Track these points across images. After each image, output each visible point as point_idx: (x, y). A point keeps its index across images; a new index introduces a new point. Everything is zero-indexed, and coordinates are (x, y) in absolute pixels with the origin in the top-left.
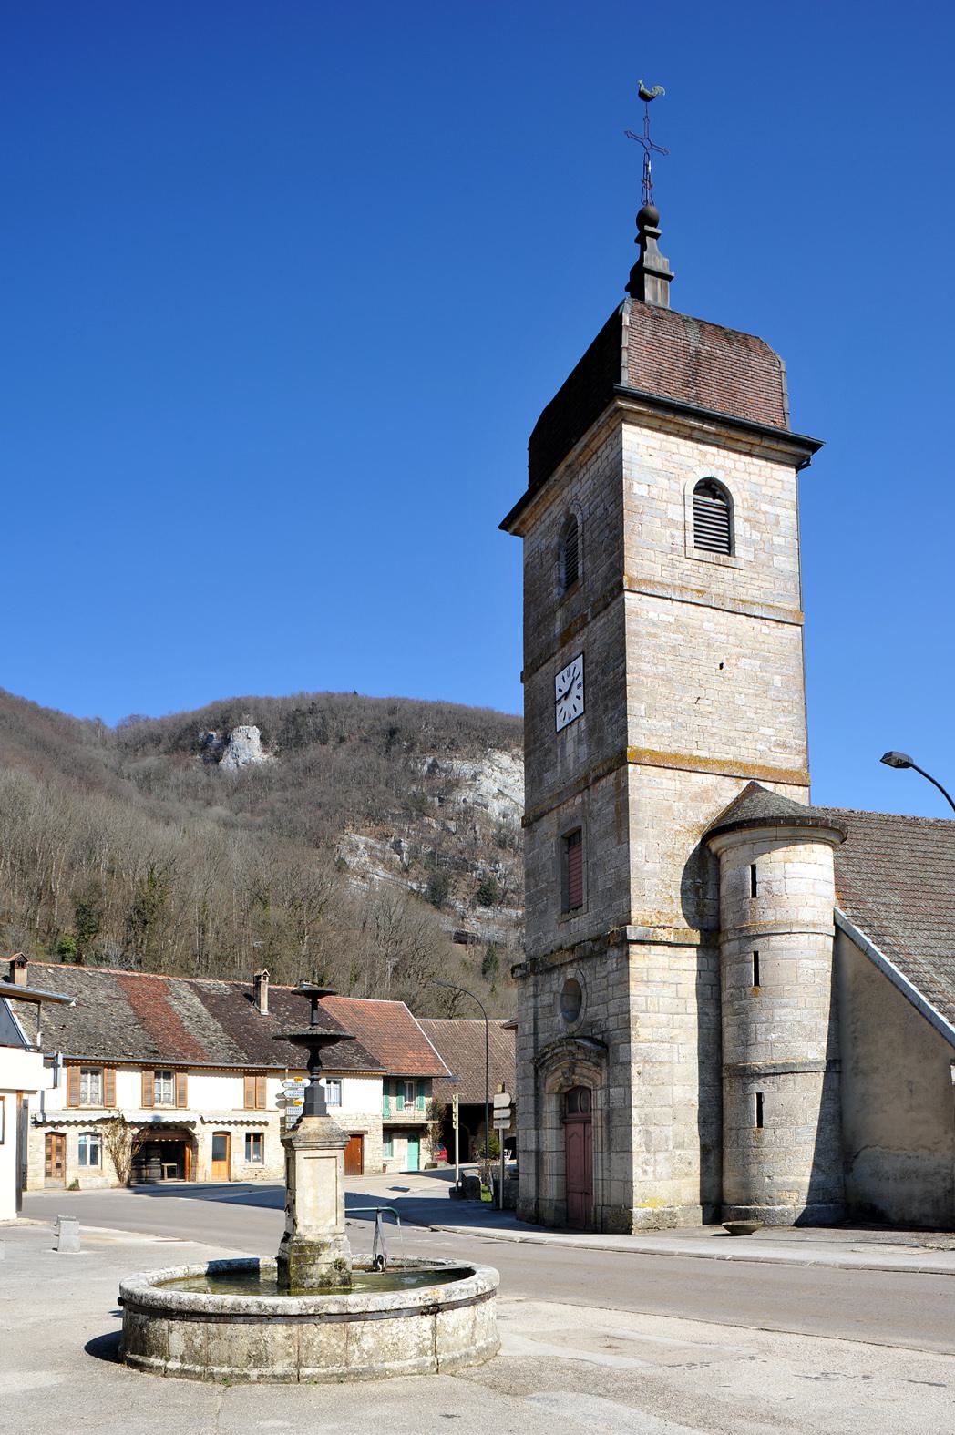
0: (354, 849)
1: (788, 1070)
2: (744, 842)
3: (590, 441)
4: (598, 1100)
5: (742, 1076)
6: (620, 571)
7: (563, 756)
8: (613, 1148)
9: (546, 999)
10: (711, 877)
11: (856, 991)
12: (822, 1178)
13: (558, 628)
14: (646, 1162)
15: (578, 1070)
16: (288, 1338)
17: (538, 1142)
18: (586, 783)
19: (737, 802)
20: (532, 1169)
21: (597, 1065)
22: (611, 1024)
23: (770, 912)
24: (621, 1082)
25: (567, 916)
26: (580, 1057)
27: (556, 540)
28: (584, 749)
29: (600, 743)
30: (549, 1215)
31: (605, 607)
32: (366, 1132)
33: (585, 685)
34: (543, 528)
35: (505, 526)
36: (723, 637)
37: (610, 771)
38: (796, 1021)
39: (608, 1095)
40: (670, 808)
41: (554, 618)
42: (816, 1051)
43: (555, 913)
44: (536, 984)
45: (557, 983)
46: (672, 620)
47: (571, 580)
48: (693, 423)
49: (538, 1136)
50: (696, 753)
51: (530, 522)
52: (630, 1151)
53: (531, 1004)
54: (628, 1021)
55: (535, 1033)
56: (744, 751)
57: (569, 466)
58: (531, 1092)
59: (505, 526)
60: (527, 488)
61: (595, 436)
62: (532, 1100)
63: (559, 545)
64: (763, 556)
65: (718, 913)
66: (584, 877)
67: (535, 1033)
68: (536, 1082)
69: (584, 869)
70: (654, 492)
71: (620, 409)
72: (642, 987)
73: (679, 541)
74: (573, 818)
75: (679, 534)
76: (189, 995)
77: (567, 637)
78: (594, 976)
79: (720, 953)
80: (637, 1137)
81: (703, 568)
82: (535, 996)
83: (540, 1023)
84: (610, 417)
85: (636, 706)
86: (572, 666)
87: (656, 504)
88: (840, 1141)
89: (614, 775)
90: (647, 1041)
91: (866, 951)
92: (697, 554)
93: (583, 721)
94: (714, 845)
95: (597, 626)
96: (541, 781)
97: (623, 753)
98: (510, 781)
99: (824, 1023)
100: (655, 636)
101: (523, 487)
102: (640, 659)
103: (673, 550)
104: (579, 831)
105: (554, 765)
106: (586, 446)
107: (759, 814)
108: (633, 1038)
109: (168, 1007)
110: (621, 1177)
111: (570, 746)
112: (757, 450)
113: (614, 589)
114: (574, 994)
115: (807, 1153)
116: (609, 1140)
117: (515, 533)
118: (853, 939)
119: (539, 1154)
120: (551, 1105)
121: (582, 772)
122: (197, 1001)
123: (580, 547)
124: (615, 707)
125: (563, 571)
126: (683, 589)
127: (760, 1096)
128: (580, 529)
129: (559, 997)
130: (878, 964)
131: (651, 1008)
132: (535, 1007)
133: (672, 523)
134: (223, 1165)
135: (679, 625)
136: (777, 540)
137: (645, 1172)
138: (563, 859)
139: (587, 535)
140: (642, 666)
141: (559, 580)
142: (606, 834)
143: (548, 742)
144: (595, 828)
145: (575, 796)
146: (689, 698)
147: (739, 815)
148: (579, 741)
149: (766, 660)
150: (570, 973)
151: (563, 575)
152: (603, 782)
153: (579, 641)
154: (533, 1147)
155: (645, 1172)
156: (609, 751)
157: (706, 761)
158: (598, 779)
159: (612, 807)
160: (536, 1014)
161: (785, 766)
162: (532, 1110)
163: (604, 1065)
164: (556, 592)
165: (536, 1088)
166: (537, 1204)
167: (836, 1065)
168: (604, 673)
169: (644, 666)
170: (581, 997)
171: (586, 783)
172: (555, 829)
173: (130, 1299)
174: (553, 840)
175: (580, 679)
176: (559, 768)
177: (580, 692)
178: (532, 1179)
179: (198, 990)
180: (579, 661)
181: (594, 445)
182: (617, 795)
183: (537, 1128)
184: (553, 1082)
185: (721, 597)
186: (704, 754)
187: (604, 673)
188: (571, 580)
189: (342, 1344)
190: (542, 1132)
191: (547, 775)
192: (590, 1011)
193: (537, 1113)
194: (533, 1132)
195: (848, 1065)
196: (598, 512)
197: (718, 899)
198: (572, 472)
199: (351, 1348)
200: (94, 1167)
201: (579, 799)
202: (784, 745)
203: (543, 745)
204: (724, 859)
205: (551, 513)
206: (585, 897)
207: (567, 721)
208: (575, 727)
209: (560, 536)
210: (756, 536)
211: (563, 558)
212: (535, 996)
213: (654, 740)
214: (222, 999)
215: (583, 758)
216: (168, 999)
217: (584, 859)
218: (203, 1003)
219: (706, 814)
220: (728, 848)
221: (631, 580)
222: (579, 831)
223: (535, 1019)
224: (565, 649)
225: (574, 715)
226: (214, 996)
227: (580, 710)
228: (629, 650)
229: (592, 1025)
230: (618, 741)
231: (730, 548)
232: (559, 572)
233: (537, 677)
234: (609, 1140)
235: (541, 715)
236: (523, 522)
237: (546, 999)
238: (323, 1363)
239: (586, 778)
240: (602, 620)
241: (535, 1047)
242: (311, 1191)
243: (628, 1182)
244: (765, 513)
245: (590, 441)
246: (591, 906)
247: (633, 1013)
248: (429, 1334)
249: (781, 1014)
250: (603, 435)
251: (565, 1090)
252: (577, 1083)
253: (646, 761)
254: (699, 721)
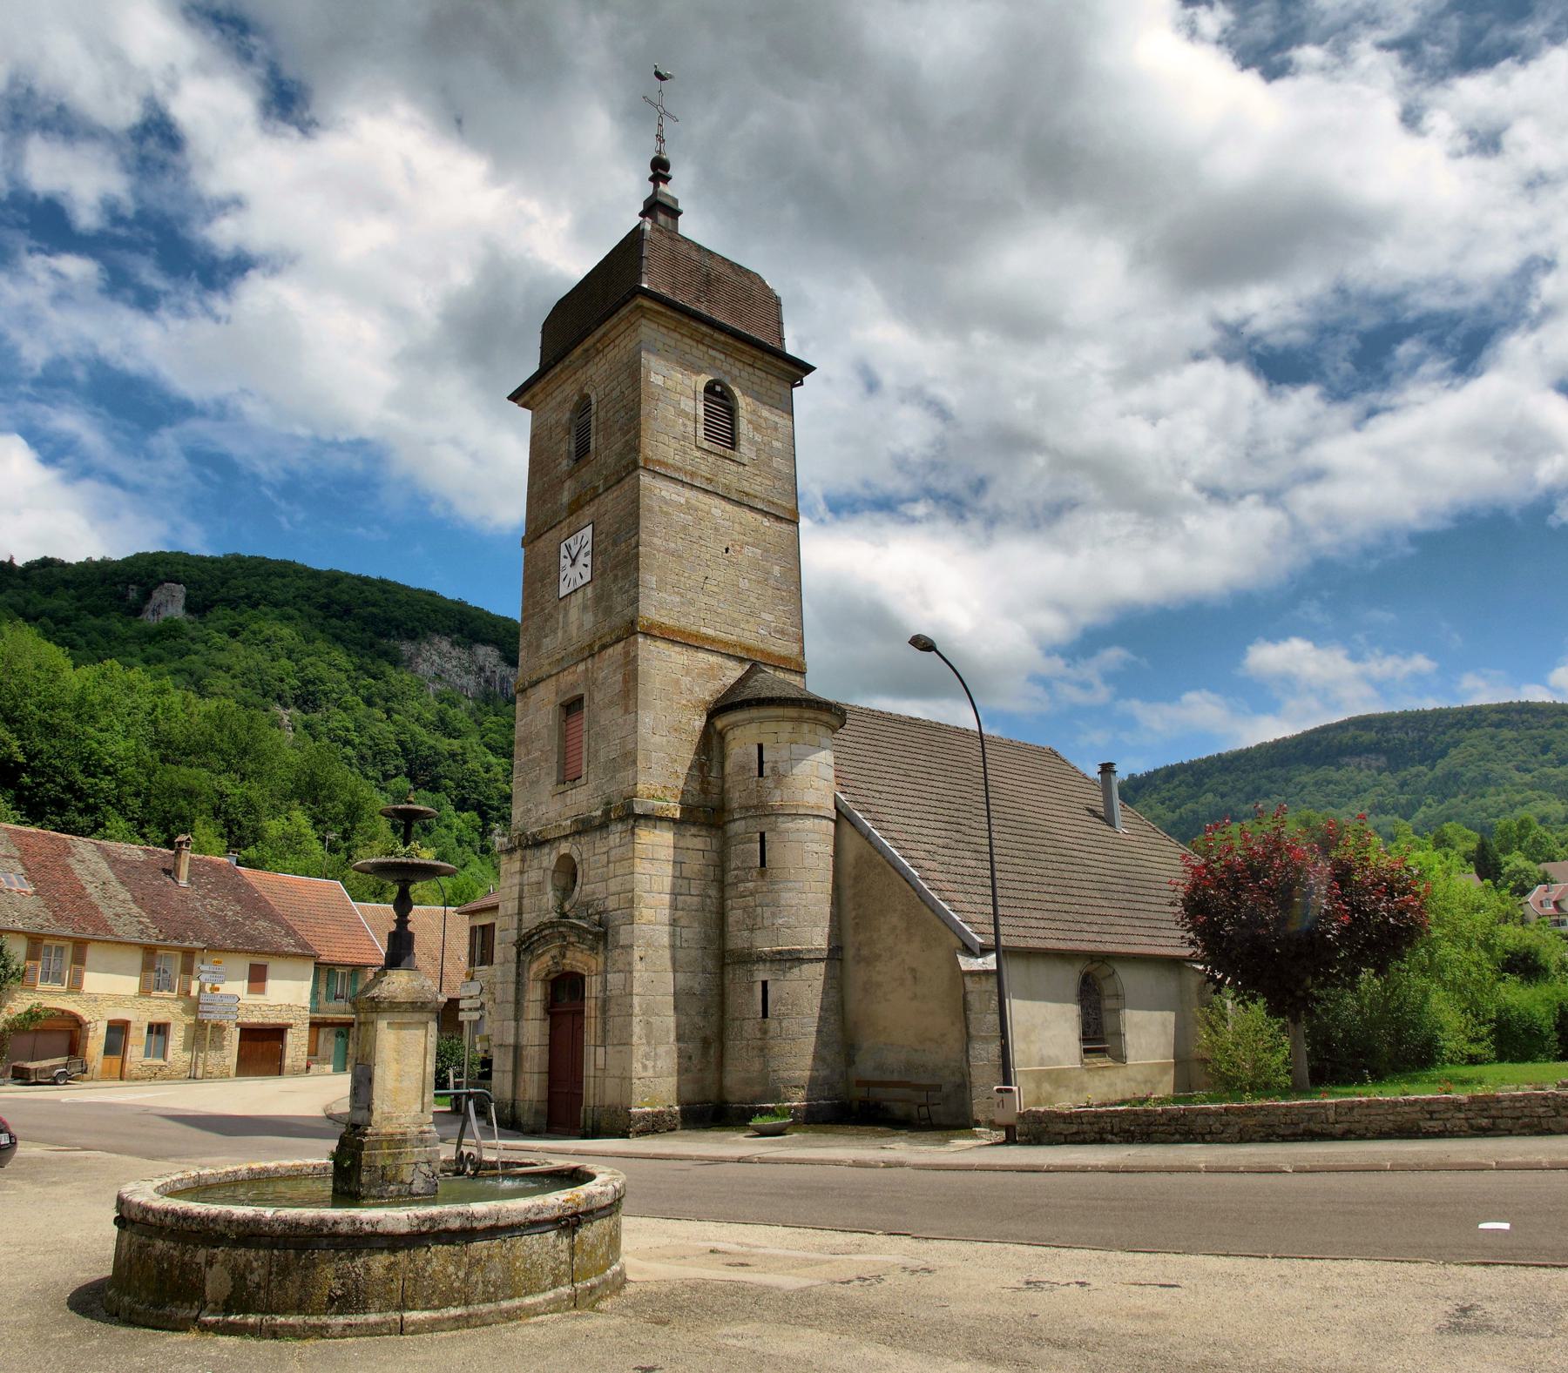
0: (276, 724)
1: (794, 959)
2: (751, 721)
3: (609, 331)
4: (593, 987)
5: (745, 962)
6: (636, 449)
7: (566, 624)
8: (609, 1041)
9: (534, 876)
10: (715, 753)
11: (862, 877)
12: (824, 1073)
13: (565, 497)
14: (646, 1056)
15: (569, 954)
16: (388, 1269)
17: (517, 1035)
18: (592, 651)
19: (741, 681)
20: (509, 1066)
21: (592, 948)
22: (612, 903)
23: (778, 792)
24: (621, 967)
25: (562, 788)
26: (572, 939)
27: (568, 415)
28: (589, 619)
29: (608, 611)
30: (526, 1118)
31: (619, 481)
32: (290, 1026)
33: (594, 554)
34: (553, 403)
35: (514, 397)
36: (727, 523)
37: (618, 641)
38: (802, 908)
39: (605, 982)
40: (677, 681)
41: (562, 488)
42: (818, 939)
43: (548, 783)
44: (523, 860)
45: (548, 858)
46: (683, 501)
47: (582, 452)
48: (704, 329)
49: (517, 1029)
50: (703, 630)
51: (541, 396)
52: (629, 1044)
53: (516, 879)
54: (632, 901)
55: (520, 913)
56: (747, 634)
57: (586, 350)
58: (512, 977)
59: (514, 397)
60: (537, 368)
61: (614, 327)
62: (512, 987)
63: (571, 420)
64: (763, 456)
65: (723, 791)
66: (585, 746)
67: (520, 913)
68: (518, 968)
69: (585, 738)
70: (669, 383)
71: (640, 307)
72: (647, 865)
73: (690, 429)
74: (573, 686)
75: (691, 424)
76: (95, 859)
77: (576, 506)
78: (590, 854)
79: (724, 832)
80: (637, 1029)
81: (711, 459)
82: (522, 872)
83: (526, 902)
84: (631, 312)
85: (649, 578)
86: (579, 535)
87: (669, 394)
88: (842, 1030)
89: (622, 644)
90: (650, 923)
91: (867, 836)
92: (706, 445)
93: (589, 589)
94: (720, 724)
95: (609, 500)
96: (538, 647)
97: (633, 623)
98: (448, 666)
99: (827, 909)
100: (667, 513)
101: (533, 367)
102: (653, 534)
103: (684, 438)
104: (580, 699)
105: (555, 631)
106: (605, 335)
107: (765, 694)
108: (636, 919)
109: (67, 870)
110: (618, 1073)
111: (574, 614)
112: (759, 364)
113: (630, 464)
114: (568, 872)
115: (809, 1044)
116: (604, 1031)
117: (524, 406)
118: (854, 823)
119: (517, 1049)
120: (535, 994)
121: (587, 640)
122: (104, 866)
123: (593, 424)
124: (625, 577)
125: (573, 445)
126: (693, 475)
127: (765, 984)
128: (594, 407)
129: (549, 873)
130: (880, 850)
131: (655, 888)
132: (521, 885)
133: (687, 415)
134: (116, 1061)
135: (689, 508)
136: (776, 444)
137: (645, 1067)
138: (560, 726)
139: (602, 414)
140: (656, 541)
141: (569, 452)
142: (612, 703)
143: (549, 608)
144: (598, 697)
145: (577, 664)
146: (698, 576)
147: (747, 694)
148: (585, 608)
149: (766, 551)
150: (565, 848)
151: (573, 448)
152: (610, 651)
153: (589, 511)
154: (511, 1040)
155: (645, 1067)
156: (617, 620)
157: (713, 640)
158: (604, 647)
159: (619, 677)
160: (521, 891)
161: (783, 652)
162: (512, 999)
163: (601, 948)
164: (565, 464)
165: (518, 975)
166: (513, 1106)
167: (835, 954)
168: (615, 544)
169: (656, 540)
170: (575, 875)
171: (592, 651)
172: (552, 697)
173: (144, 1218)
174: (550, 707)
175: (589, 548)
176: (560, 634)
177: (588, 560)
178: (509, 1077)
179: (106, 854)
180: (588, 531)
181: (612, 335)
182: (627, 664)
183: (517, 1019)
184: (540, 965)
185: (727, 487)
186: (710, 632)
187: (615, 544)
188: (582, 452)
189: (461, 1274)
190: (523, 1023)
191: (546, 641)
192: (586, 889)
193: (518, 1003)
194: (513, 1023)
195: (850, 953)
196: (614, 395)
197: (723, 777)
198: (587, 358)
199: (473, 1278)
200: (120, 1014)
201: (581, 667)
202: (782, 632)
203: (543, 609)
204: (730, 736)
205: (567, 391)
206: (584, 769)
207: (572, 588)
208: (580, 594)
209: (572, 412)
210: (758, 438)
211: (573, 433)
212: (522, 872)
213: (663, 612)
214: (133, 866)
215: (588, 625)
216: (70, 861)
217: (585, 727)
218: (111, 868)
219: (708, 692)
220: (735, 725)
221: (646, 460)
222: (580, 699)
223: (521, 898)
224: (573, 518)
225: (580, 582)
226: (125, 862)
227: (587, 578)
228: (642, 523)
229: (588, 905)
230: (629, 611)
231: (733, 444)
232: (568, 445)
233: (541, 544)
234: (604, 1031)
235: (542, 580)
236: (533, 397)
237: (534, 876)
238: (436, 1302)
239: (591, 646)
240: (614, 493)
241: (519, 928)
242: (394, 1067)
243: (626, 1079)
244: (766, 419)
245: (609, 331)
246: (591, 777)
247: (637, 891)
248: (565, 1256)
249: (788, 897)
250: (622, 327)
251: (552, 976)
252: (568, 968)
253: (656, 632)
254: (706, 599)
